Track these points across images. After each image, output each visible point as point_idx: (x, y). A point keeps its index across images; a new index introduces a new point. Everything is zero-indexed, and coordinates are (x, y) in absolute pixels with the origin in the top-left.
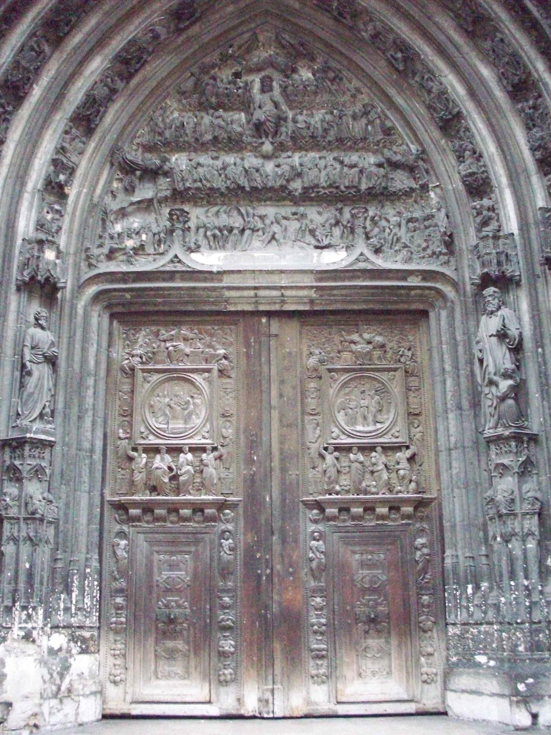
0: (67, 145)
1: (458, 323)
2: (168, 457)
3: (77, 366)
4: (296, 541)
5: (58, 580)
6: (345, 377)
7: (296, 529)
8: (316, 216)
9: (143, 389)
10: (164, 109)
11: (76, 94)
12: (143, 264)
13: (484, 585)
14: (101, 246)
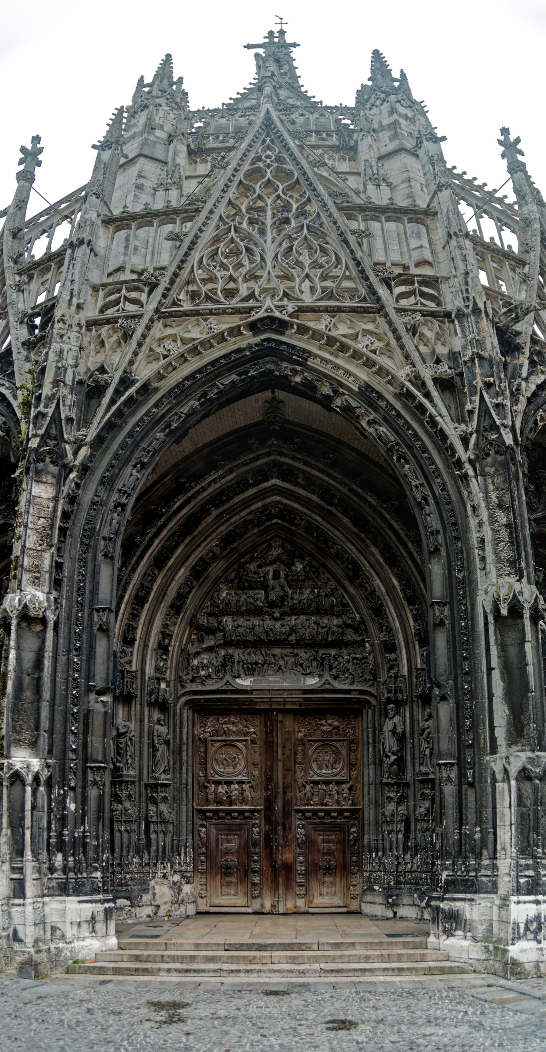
0: (168, 622)
1: (376, 718)
2: (225, 786)
3: (178, 741)
4: (290, 829)
5: (175, 850)
6: (317, 744)
7: (290, 824)
8: (303, 654)
9: (211, 751)
10: (218, 591)
11: (172, 592)
12: (211, 685)
13: (380, 853)
14: (187, 674)
